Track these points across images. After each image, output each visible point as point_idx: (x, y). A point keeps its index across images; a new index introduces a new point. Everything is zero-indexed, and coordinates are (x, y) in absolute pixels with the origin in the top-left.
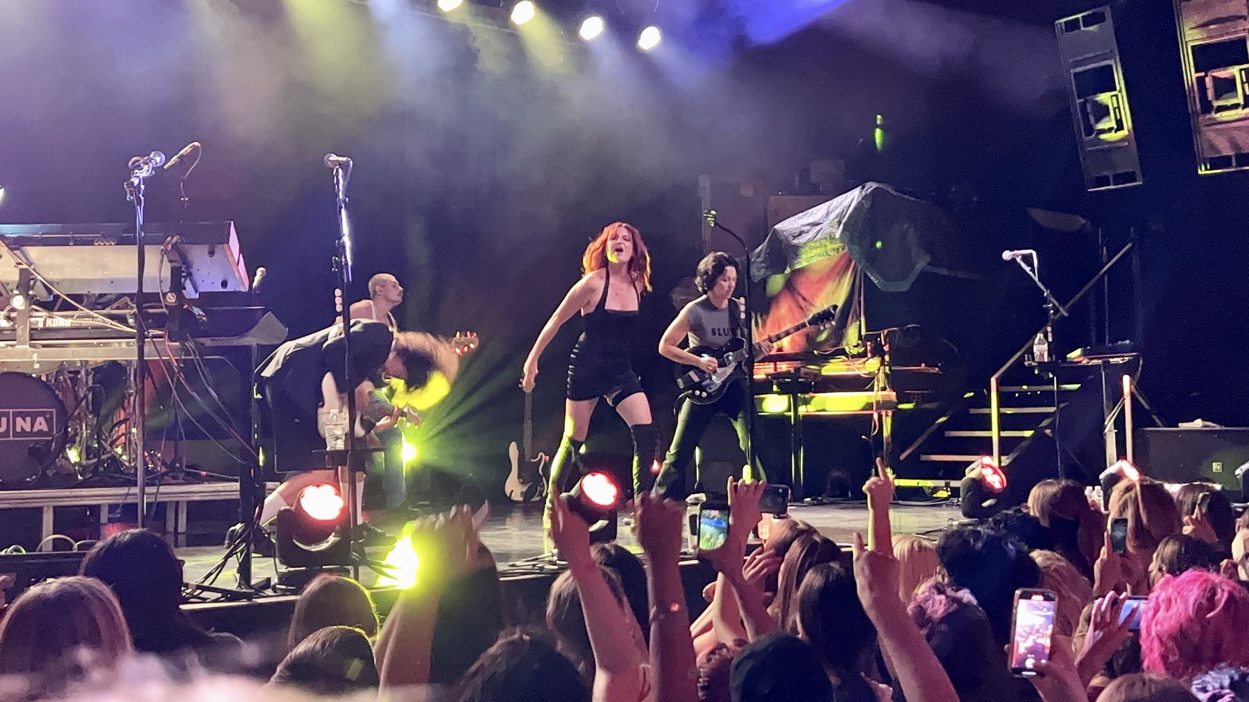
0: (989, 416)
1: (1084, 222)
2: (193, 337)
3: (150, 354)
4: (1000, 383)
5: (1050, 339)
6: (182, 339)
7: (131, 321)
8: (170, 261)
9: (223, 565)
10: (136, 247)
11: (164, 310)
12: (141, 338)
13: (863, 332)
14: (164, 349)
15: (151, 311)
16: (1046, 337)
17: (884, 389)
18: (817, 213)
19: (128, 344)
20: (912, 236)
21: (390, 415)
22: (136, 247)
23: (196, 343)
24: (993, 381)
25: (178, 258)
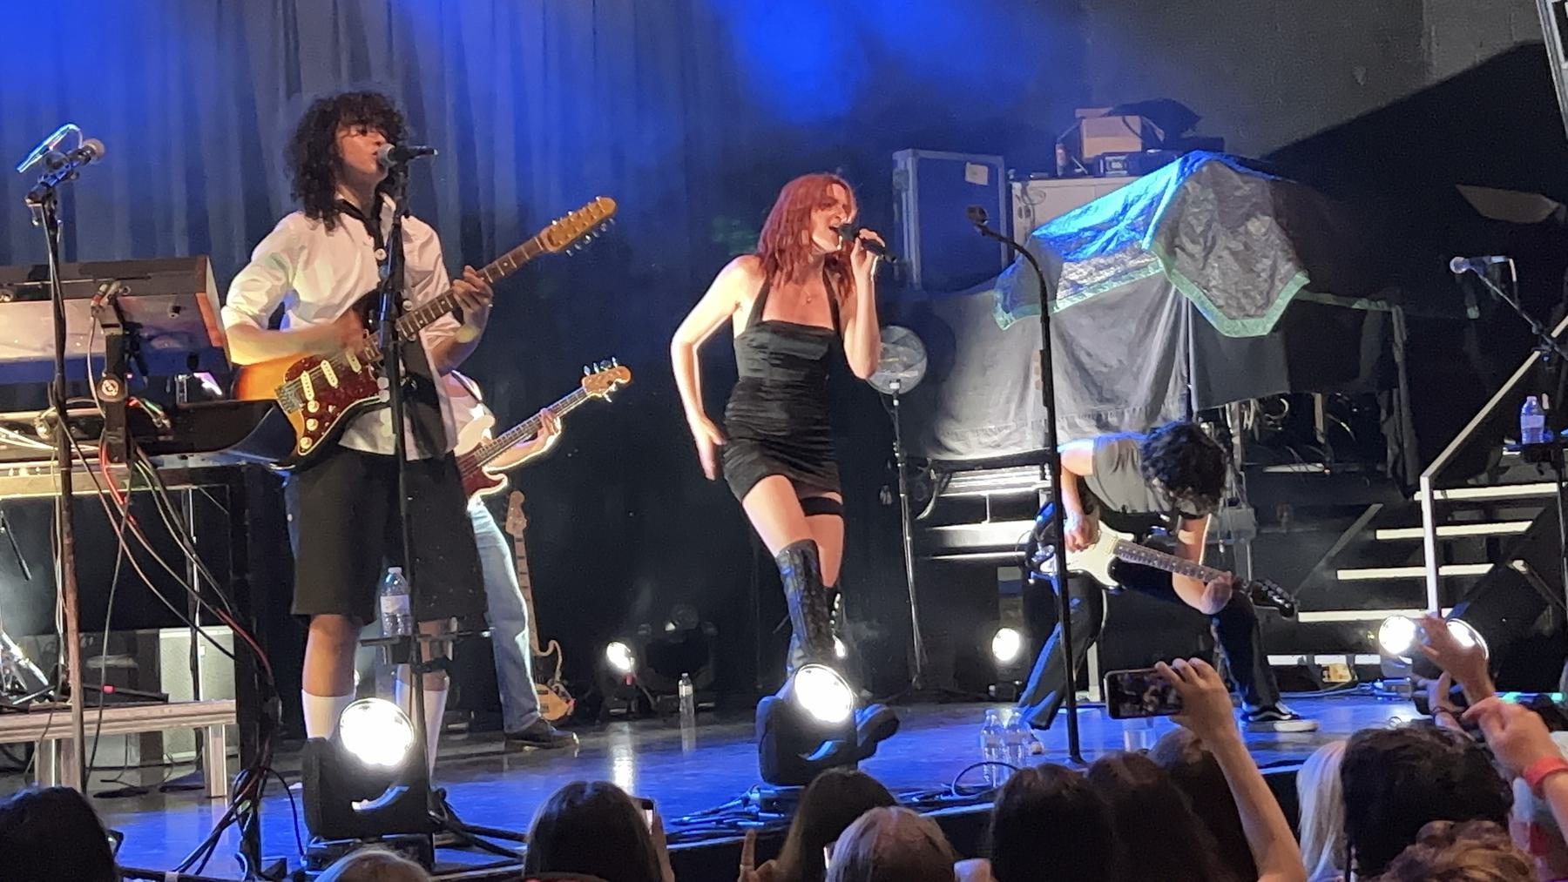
0: (1421, 541)
1: (1554, 205)
2: (149, 453)
3: (83, 487)
4: (1435, 486)
5: (1546, 406)
6: (129, 457)
7: (42, 431)
8: (104, 326)
9: (215, 839)
10: (51, 304)
11: (99, 410)
12: (67, 459)
13: (1195, 408)
14: (104, 478)
15: (71, 412)
16: (1540, 401)
17: (1233, 503)
18: (1106, 207)
19: (32, 471)
20: (1277, 237)
21: (871, 536)
22: (51, 304)
23: (155, 466)
24: (1424, 481)
25: (115, 320)
